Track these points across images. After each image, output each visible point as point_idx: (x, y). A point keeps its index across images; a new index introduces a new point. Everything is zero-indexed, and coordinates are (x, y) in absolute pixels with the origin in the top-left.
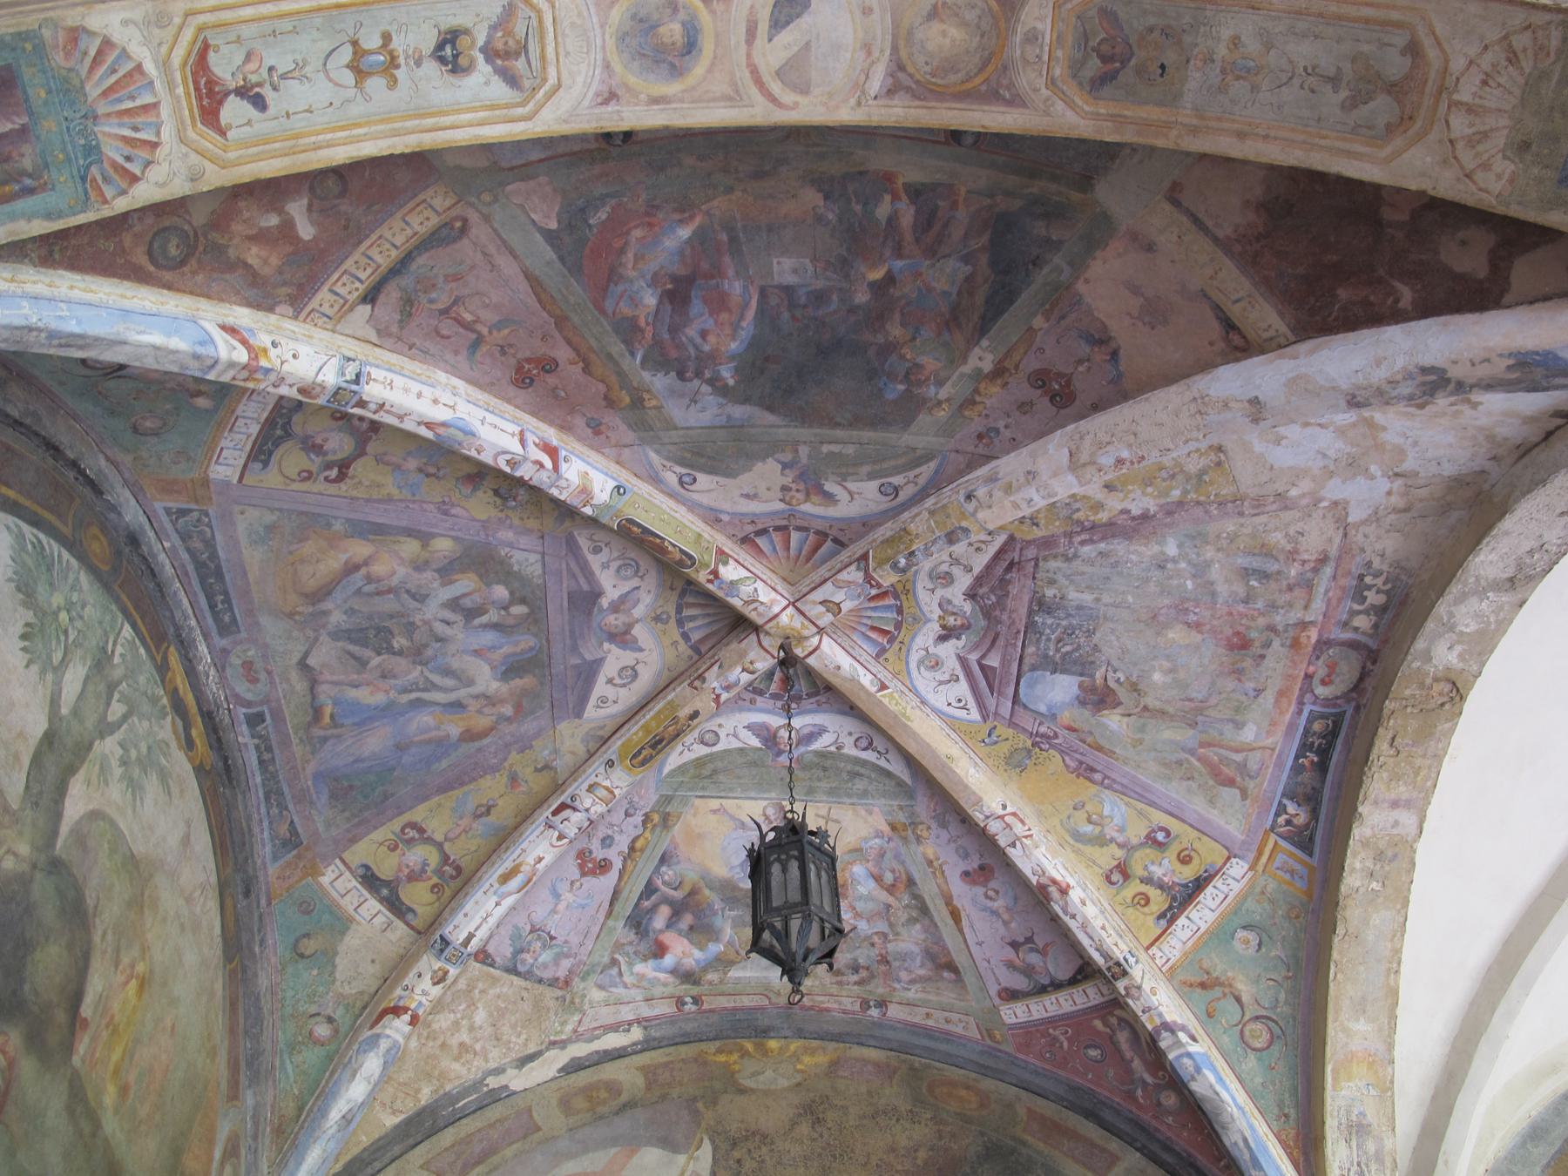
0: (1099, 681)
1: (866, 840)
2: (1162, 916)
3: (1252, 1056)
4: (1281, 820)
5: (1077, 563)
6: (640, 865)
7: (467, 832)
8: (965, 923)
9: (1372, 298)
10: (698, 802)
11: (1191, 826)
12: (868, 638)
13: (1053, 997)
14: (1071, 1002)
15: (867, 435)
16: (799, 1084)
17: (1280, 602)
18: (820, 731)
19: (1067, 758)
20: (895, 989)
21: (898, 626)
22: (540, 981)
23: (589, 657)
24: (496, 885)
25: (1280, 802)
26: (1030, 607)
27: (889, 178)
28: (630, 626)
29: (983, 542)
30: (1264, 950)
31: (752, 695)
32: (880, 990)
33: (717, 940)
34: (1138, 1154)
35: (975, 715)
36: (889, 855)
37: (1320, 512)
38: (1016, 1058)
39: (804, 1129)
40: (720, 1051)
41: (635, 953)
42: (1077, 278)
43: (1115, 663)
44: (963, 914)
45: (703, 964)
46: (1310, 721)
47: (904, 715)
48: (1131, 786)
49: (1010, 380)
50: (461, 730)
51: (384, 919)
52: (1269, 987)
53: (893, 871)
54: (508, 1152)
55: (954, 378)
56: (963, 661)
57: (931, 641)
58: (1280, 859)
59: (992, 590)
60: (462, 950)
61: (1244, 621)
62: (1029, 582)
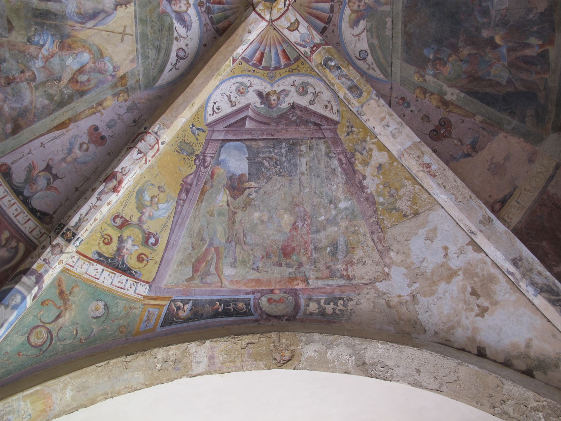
0: (247, 185)
1: (111, 60)
2: (100, 255)
3: (24, 338)
4: (180, 304)
5: (326, 159)
8: (57, 133)
9: (550, 256)
11: (163, 256)
13: (15, 201)
14: (16, 213)
15: (399, 41)
17: (318, 265)
18: (188, 27)
21: (266, 68)
25: (190, 300)
26: (291, 139)
27: (551, 42)
29: (332, 108)
30: (95, 320)
35: (210, 119)
36: (101, 76)
37: (380, 269)
42: (506, 132)
43: (262, 191)
44: (64, 131)
46: (243, 300)
47: (218, 75)
48: (181, 216)
49: (442, 109)
52: (72, 332)
53: (89, 80)
55: (439, 82)
56: (247, 107)
57: (257, 88)
58: (156, 311)
59: (298, 117)
61: (302, 251)
62: (308, 136)
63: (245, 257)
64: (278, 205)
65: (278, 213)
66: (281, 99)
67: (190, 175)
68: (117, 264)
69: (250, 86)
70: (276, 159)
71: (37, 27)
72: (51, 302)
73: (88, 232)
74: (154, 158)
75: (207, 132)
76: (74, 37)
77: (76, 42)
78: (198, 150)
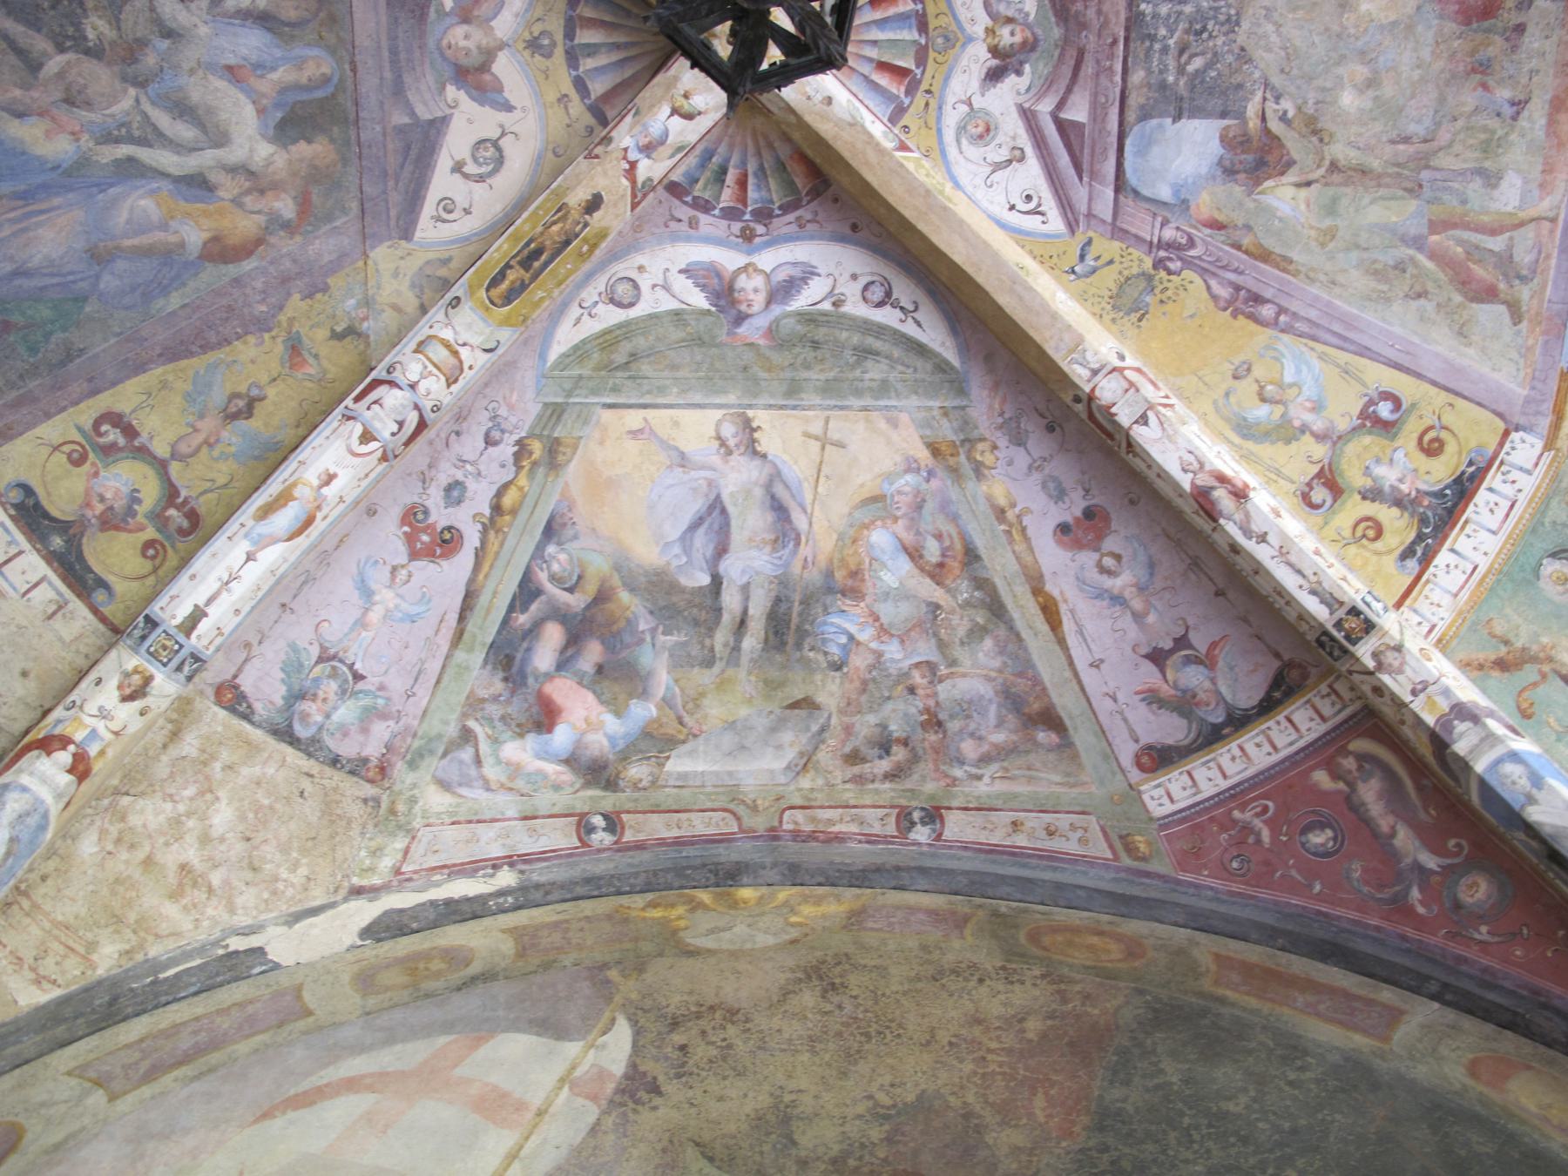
0: (1253, 124)
1: (889, 477)
2: (1408, 553)
6: (510, 542)
7: (210, 446)
8: (1068, 626)
10: (607, 415)
11: (1434, 383)
12: (875, 86)
13: (1234, 745)
14: (1267, 748)
16: (794, 942)
19: (1213, 283)
20: (955, 779)
21: (921, 58)
22: (335, 762)
23: (424, 114)
24: (250, 523)
28: (489, 55)
31: (692, 212)
32: (930, 787)
33: (644, 694)
34: (1436, 1005)
35: (1056, 223)
36: (930, 506)
38: (1179, 882)
39: (808, 998)
40: (653, 905)
41: (503, 718)
43: (1276, 80)
44: (1063, 608)
45: (621, 745)
47: (942, 192)
48: (1324, 322)
50: (206, 235)
51: (51, 595)
53: (939, 537)
54: (243, 1048)
56: (1028, 116)
57: (975, 85)
60: (181, 638)
63: (1471, 141)
64: (1327, 29)
65: (1352, 31)
66: (1010, 13)
67: (1208, 288)
68: (1439, 511)
69: (970, 105)
70: (1187, 32)
71: (806, 646)
72: (1526, 695)
73: (1350, 577)
74: (1160, 384)
75: (1091, 234)
76: (831, 560)
77: (842, 560)
78: (1141, 260)
